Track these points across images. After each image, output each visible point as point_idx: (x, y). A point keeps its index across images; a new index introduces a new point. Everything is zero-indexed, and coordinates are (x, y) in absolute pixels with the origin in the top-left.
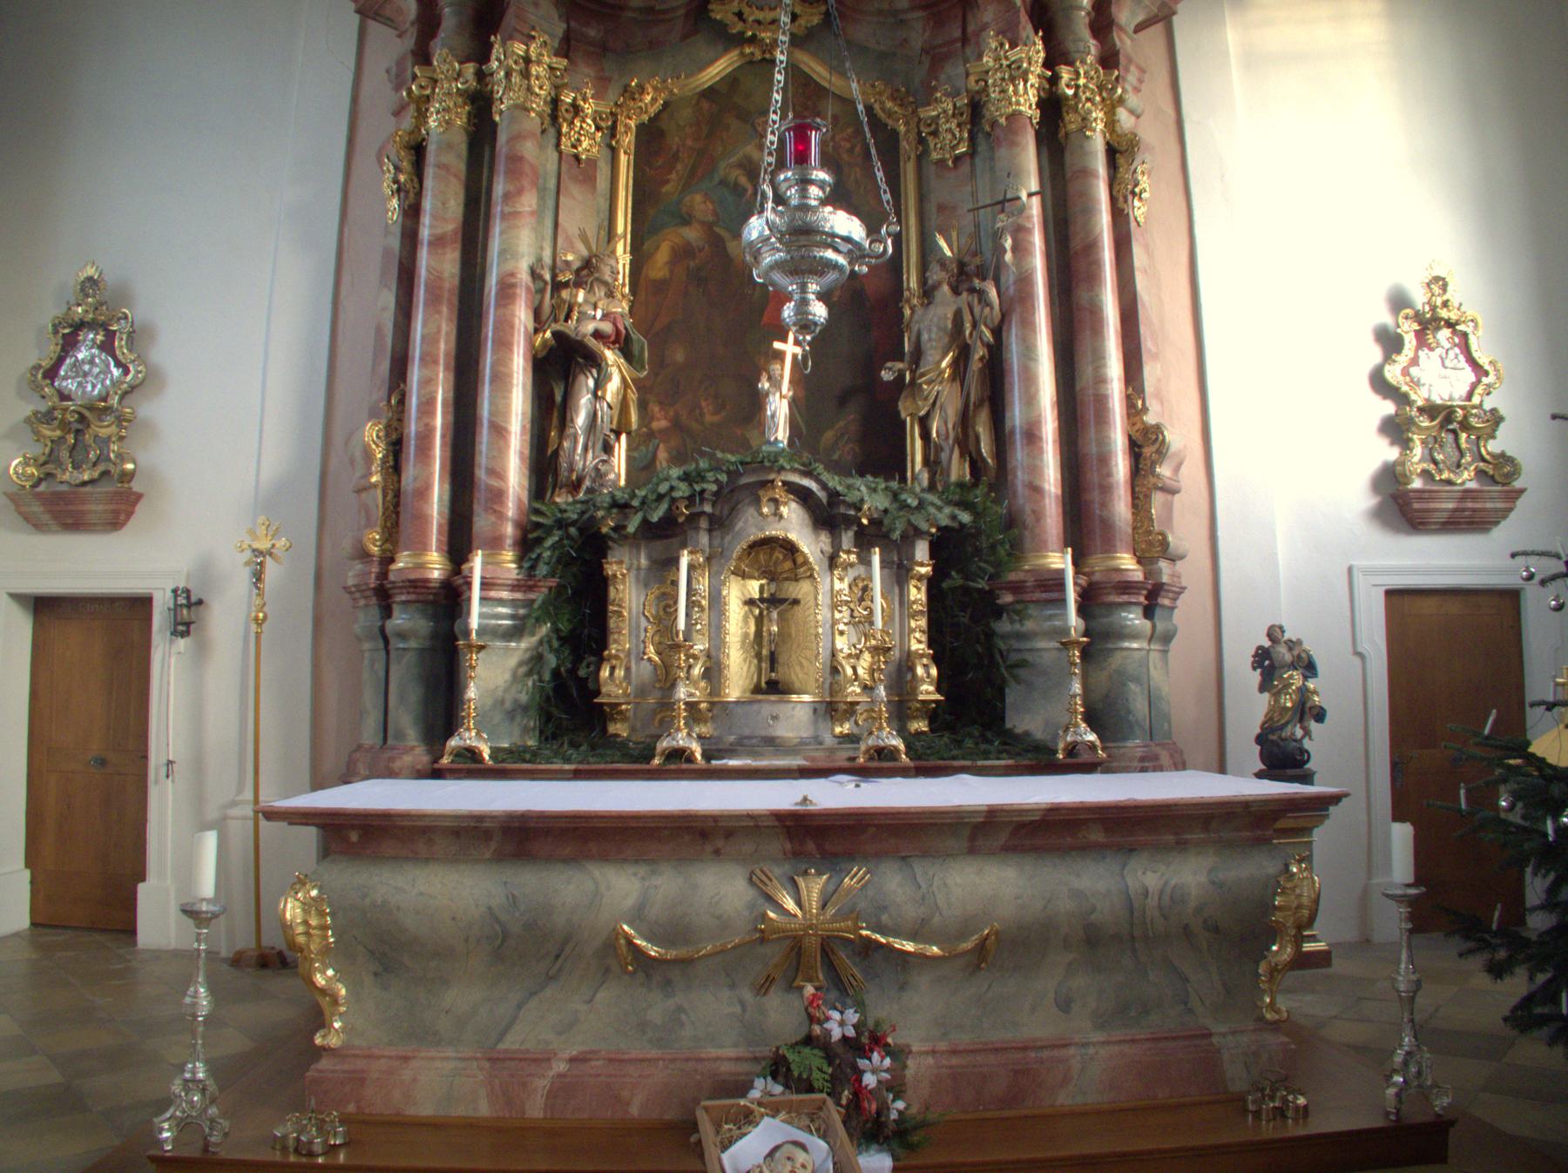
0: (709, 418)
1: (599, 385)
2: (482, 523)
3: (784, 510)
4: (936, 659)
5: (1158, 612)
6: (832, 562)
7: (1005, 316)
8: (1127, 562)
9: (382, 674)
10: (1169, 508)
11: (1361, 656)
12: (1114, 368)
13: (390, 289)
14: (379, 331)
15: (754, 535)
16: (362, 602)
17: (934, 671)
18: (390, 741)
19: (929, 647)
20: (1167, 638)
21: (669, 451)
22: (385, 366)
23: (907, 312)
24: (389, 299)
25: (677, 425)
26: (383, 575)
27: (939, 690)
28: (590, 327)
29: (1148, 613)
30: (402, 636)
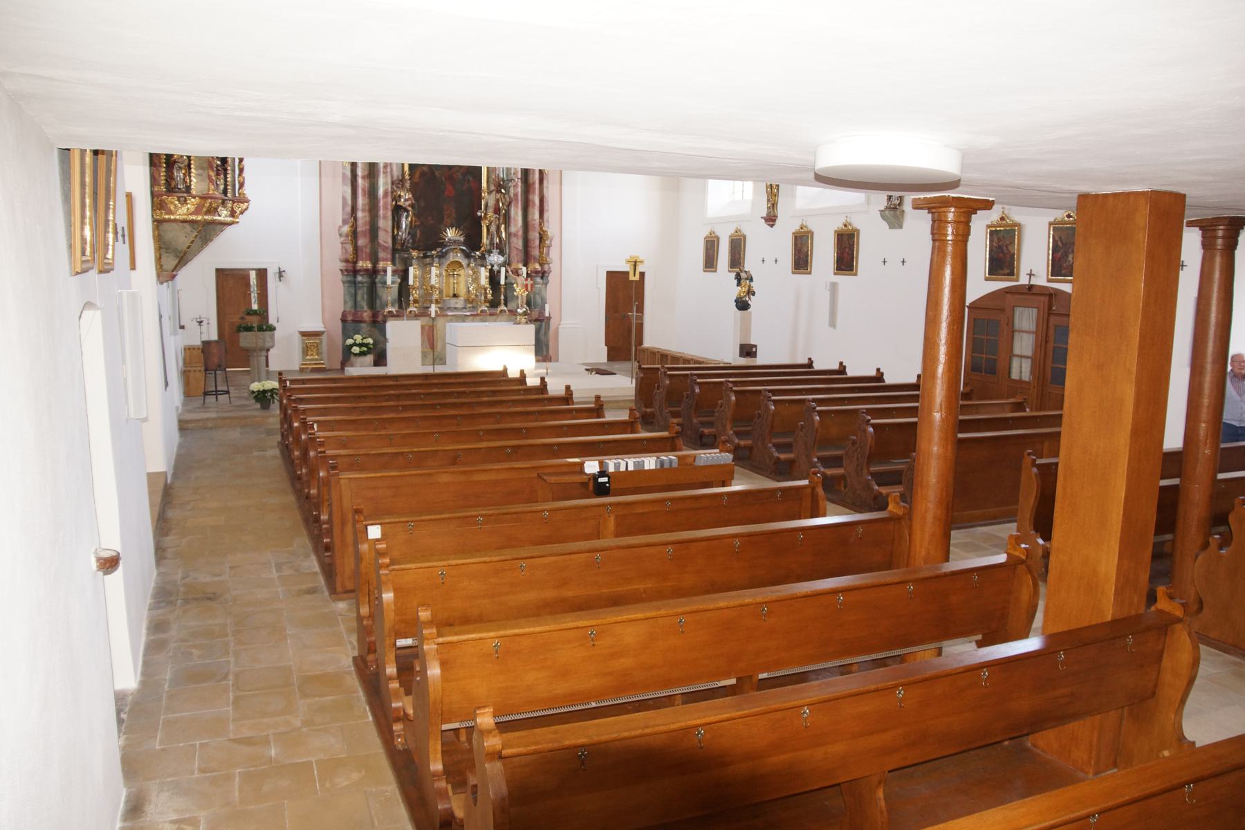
0: (431, 222)
1: (407, 218)
2: (381, 254)
3: (459, 255)
4: (491, 289)
5: (544, 278)
6: (468, 265)
7: (510, 203)
8: (537, 266)
9: (353, 292)
10: (548, 251)
11: (599, 288)
12: (537, 216)
13: (347, 186)
14: (344, 199)
15: (452, 260)
16: (346, 273)
17: (491, 292)
18: (359, 309)
19: (490, 285)
20: (546, 284)
21: (420, 231)
22: (349, 209)
23: (483, 195)
24: (348, 190)
25: (422, 223)
26: (354, 267)
27: (492, 296)
28: (408, 203)
29: (542, 278)
30: (360, 282)
